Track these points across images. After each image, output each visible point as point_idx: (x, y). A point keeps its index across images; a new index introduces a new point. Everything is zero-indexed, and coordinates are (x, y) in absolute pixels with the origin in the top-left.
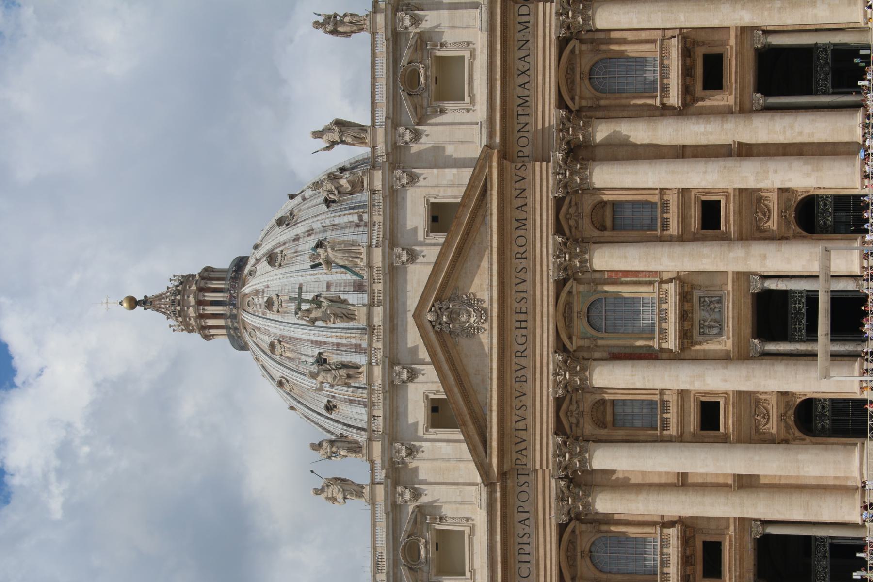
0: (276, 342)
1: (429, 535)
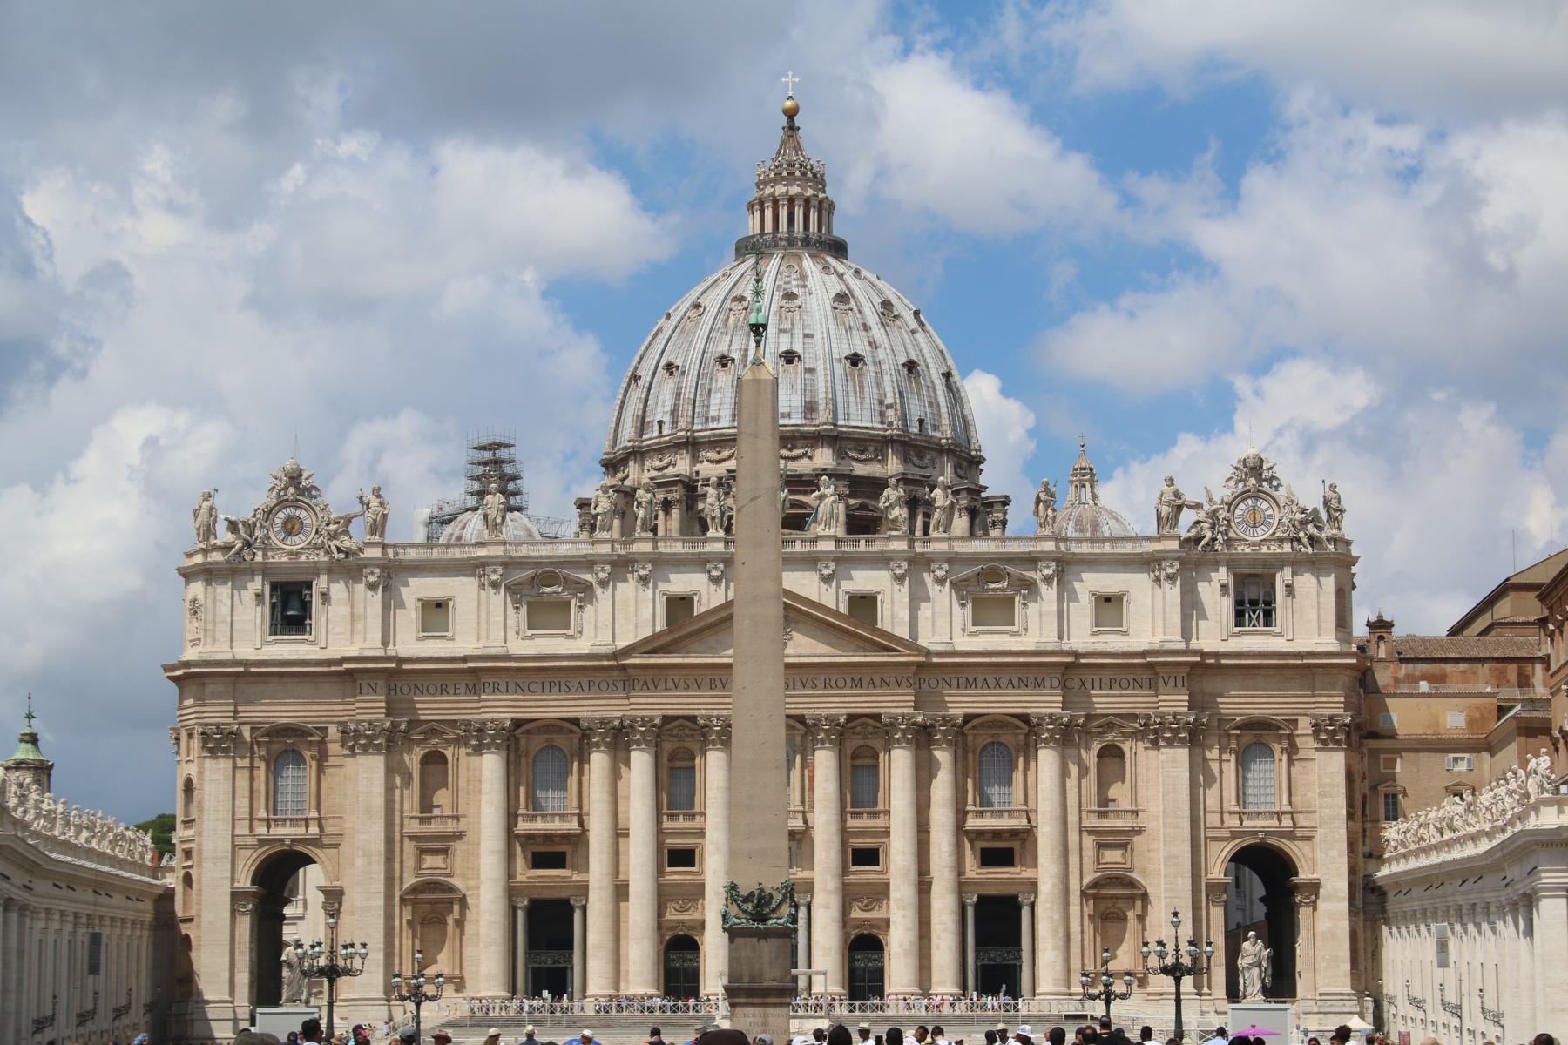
1: (565, 595)
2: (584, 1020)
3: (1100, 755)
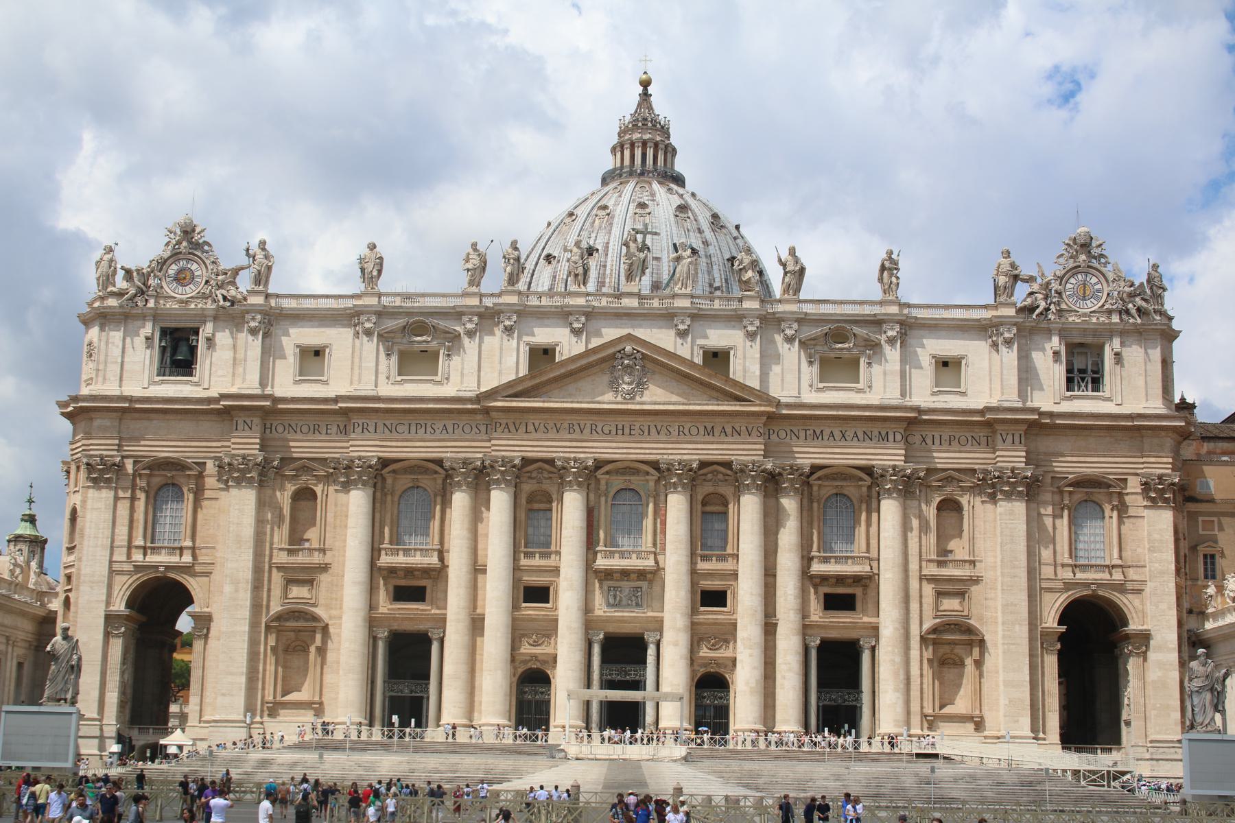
0: (608, 211)
2: (433, 747)
3: (939, 508)
